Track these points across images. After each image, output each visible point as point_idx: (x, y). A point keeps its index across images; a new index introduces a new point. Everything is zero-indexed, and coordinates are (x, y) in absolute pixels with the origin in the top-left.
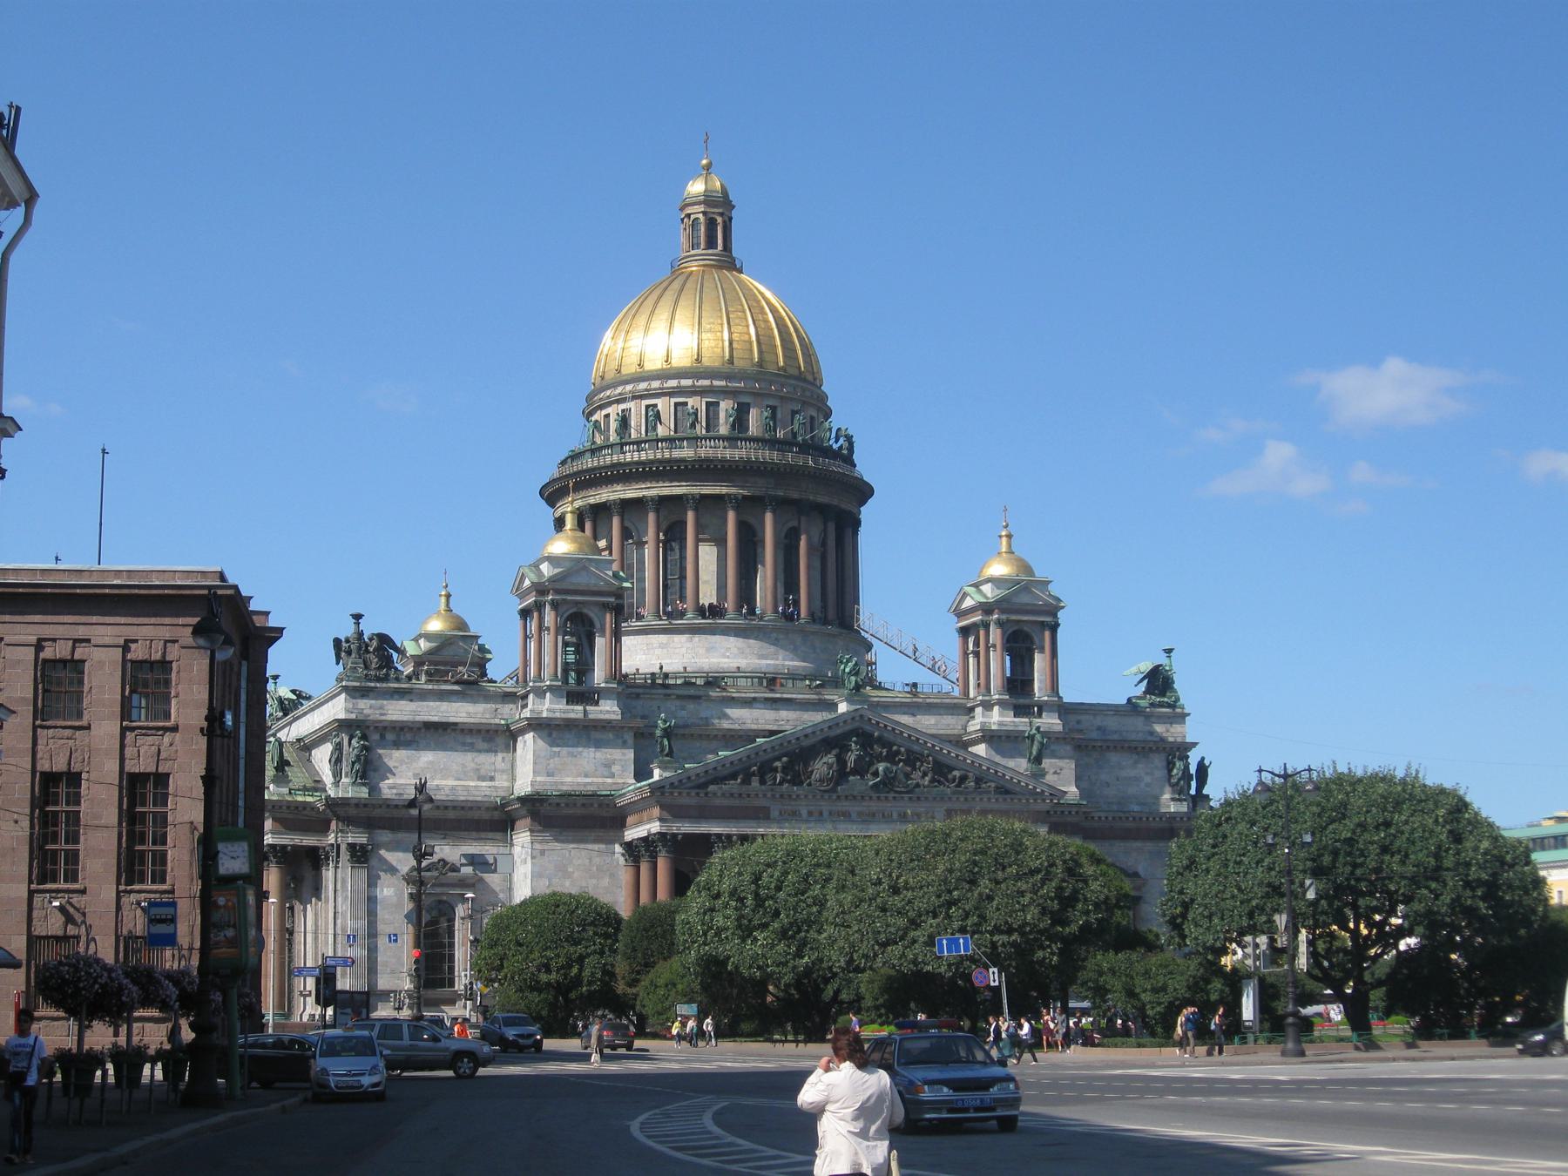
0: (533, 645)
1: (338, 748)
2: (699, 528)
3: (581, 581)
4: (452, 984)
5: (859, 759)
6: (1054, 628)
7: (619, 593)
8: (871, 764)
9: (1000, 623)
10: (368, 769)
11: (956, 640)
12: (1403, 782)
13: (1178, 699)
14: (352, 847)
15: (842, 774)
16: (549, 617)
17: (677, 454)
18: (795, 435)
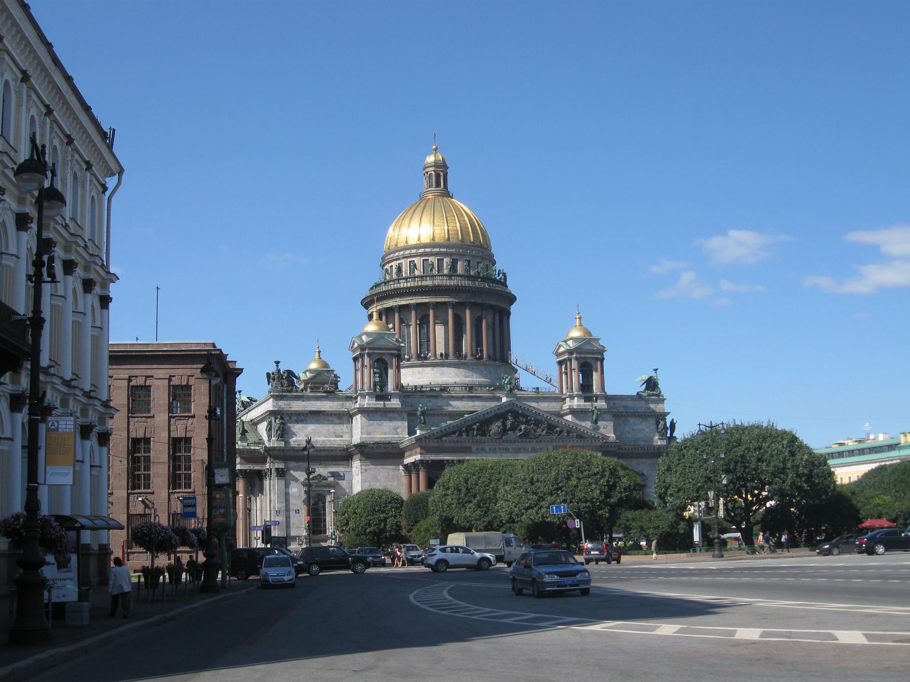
0: (359, 374)
1: (270, 423)
2: (435, 318)
3: (381, 343)
4: (325, 533)
5: (512, 423)
6: (602, 360)
7: (399, 349)
8: (518, 425)
9: (576, 359)
10: (284, 433)
11: (557, 367)
12: (767, 428)
14: (277, 469)
15: (504, 431)
16: (367, 361)
17: (424, 283)
18: (479, 273)
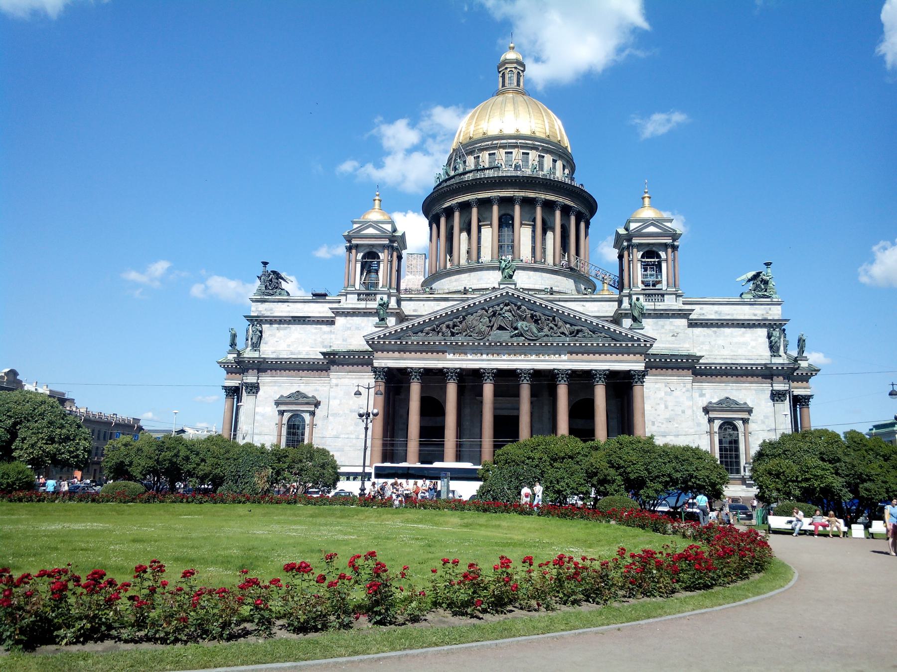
3: (371, 231)
6: (675, 248)
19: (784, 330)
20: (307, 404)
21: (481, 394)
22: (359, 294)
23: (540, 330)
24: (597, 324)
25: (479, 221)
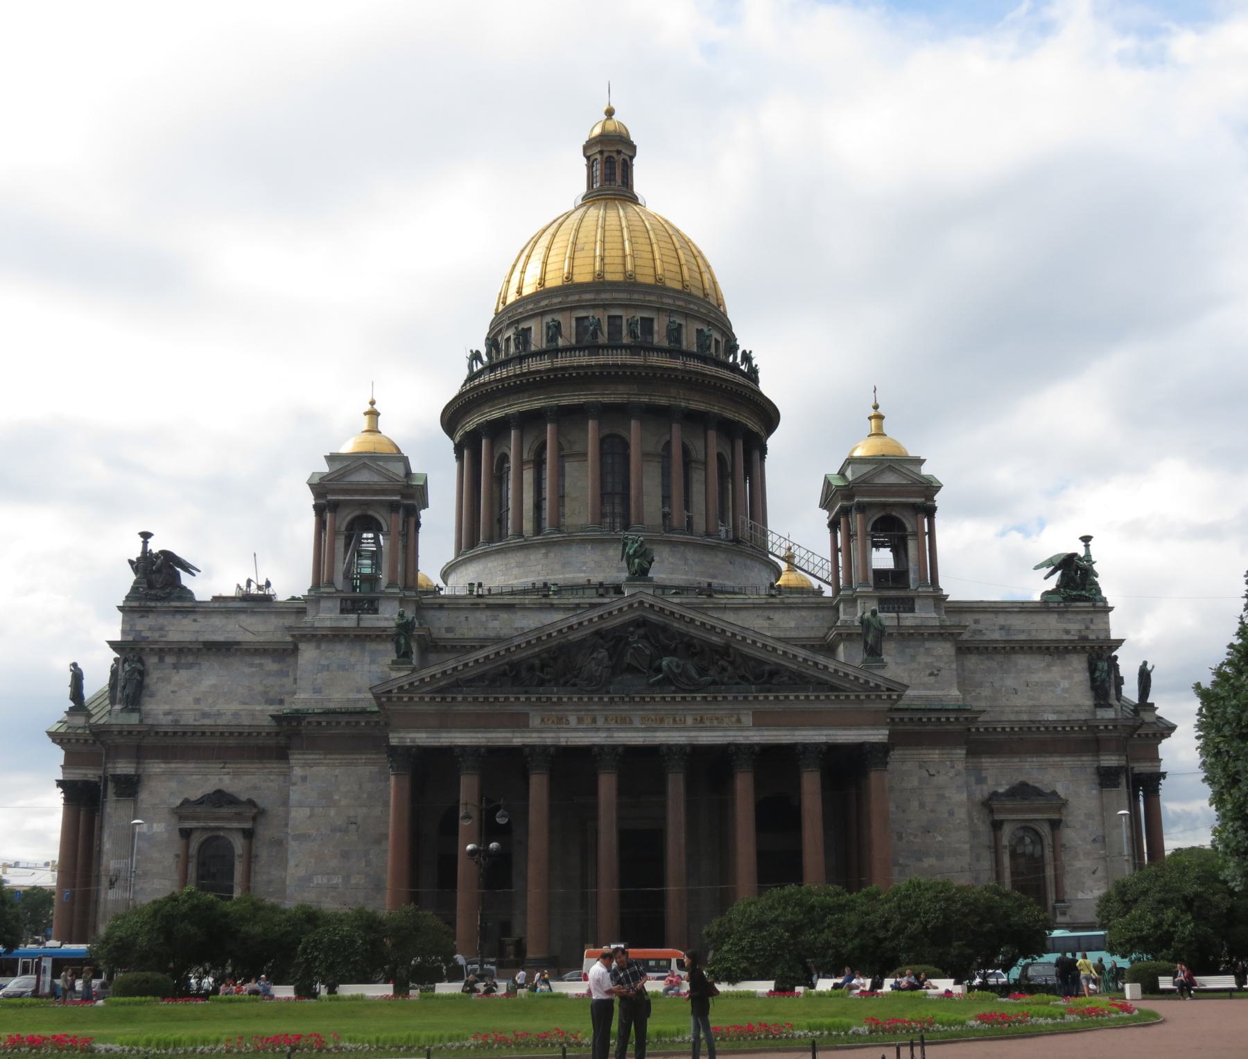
3: (364, 477)
6: (930, 512)
9: (862, 508)
13: (1099, 591)
14: (118, 779)
19: (1116, 657)
20: (239, 817)
21: (594, 791)
22: (343, 600)
23: (702, 671)
24: (805, 660)
25: (560, 448)
